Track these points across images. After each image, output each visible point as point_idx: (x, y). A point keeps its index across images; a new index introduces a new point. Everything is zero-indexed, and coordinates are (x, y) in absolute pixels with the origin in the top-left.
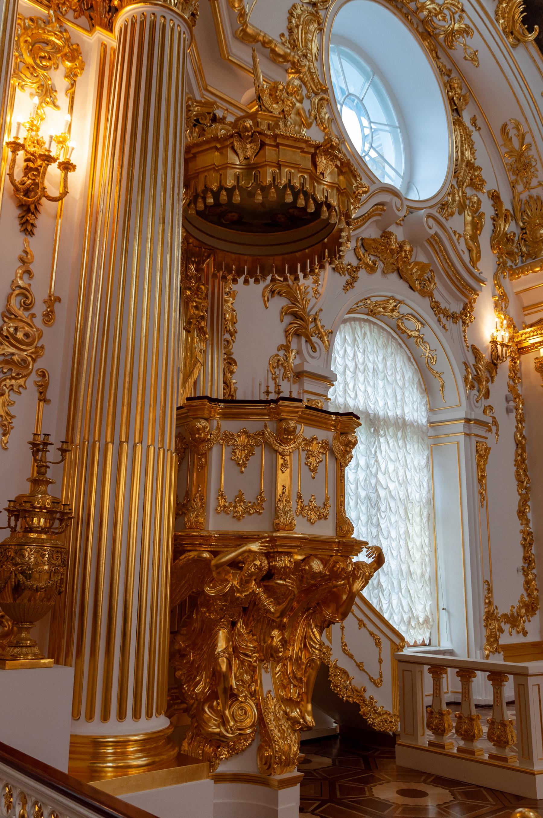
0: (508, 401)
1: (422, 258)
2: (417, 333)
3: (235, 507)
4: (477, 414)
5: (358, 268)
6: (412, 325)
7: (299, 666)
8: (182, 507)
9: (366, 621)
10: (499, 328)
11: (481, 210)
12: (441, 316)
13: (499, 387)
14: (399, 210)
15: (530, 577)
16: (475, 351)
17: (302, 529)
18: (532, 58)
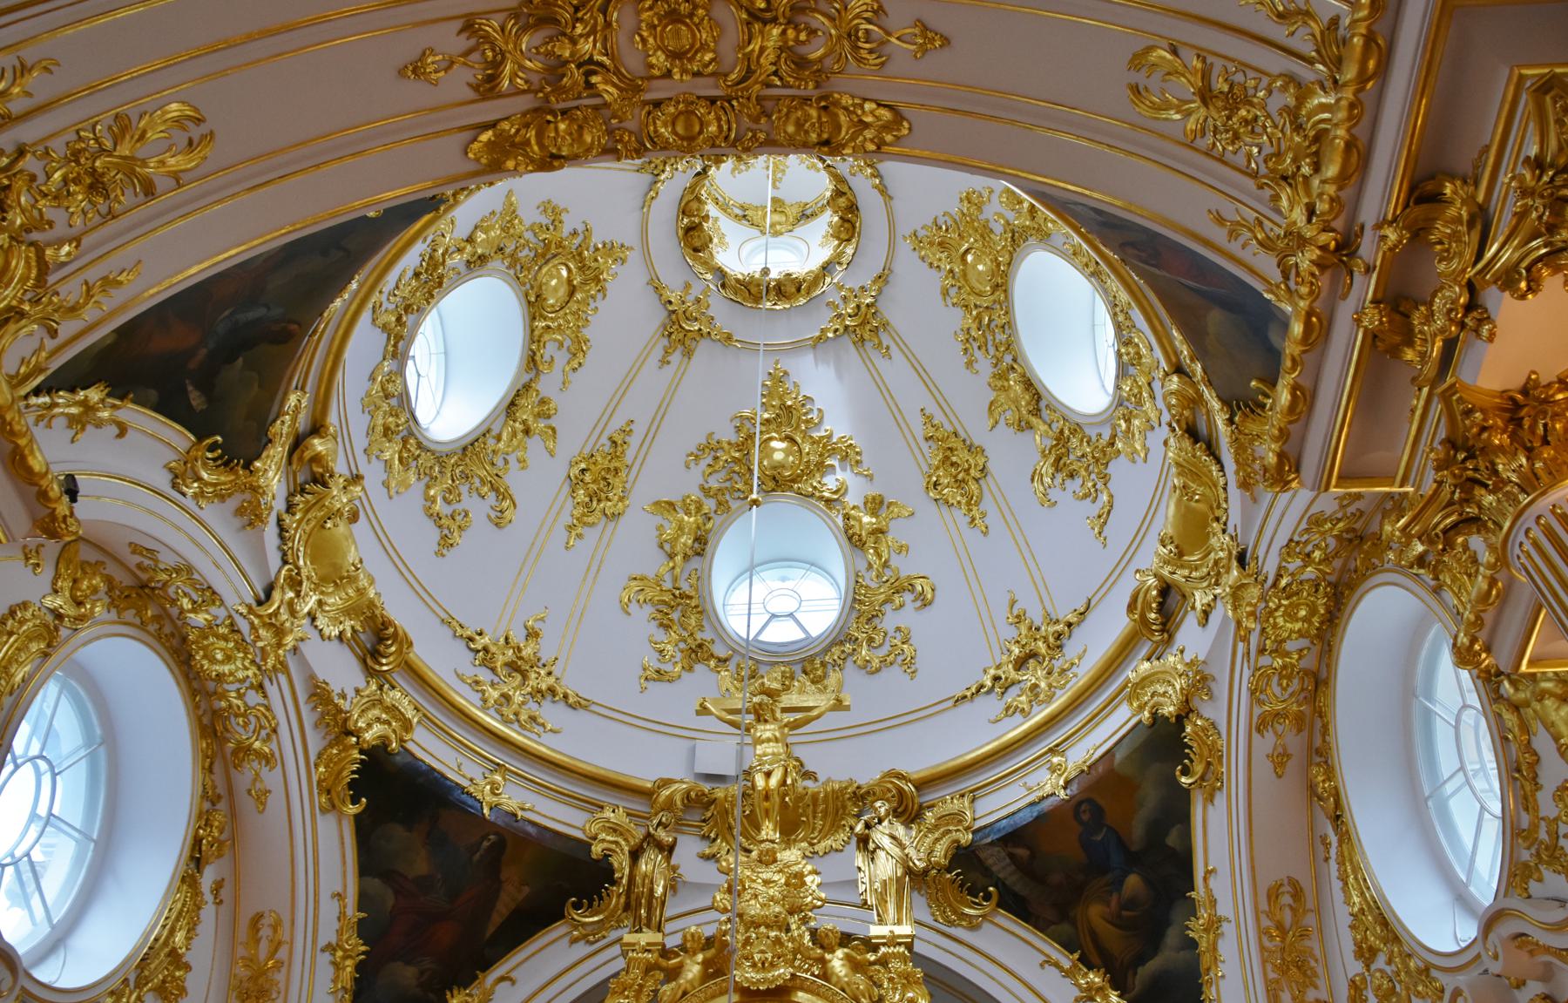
18: (342, 838)
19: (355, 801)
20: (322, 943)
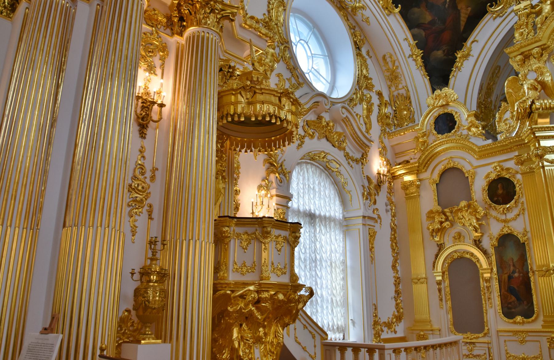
0: (387, 205)
1: (339, 130)
2: (337, 170)
3: (242, 269)
4: (370, 213)
5: (304, 136)
6: (334, 165)
7: (272, 346)
8: (217, 269)
9: (307, 325)
10: (382, 165)
11: (372, 102)
12: (350, 160)
13: (382, 198)
14: (326, 105)
15: (399, 301)
16: (369, 179)
17: (274, 279)
18: (398, 21)
19: (397, 7)
20: (407, 55)
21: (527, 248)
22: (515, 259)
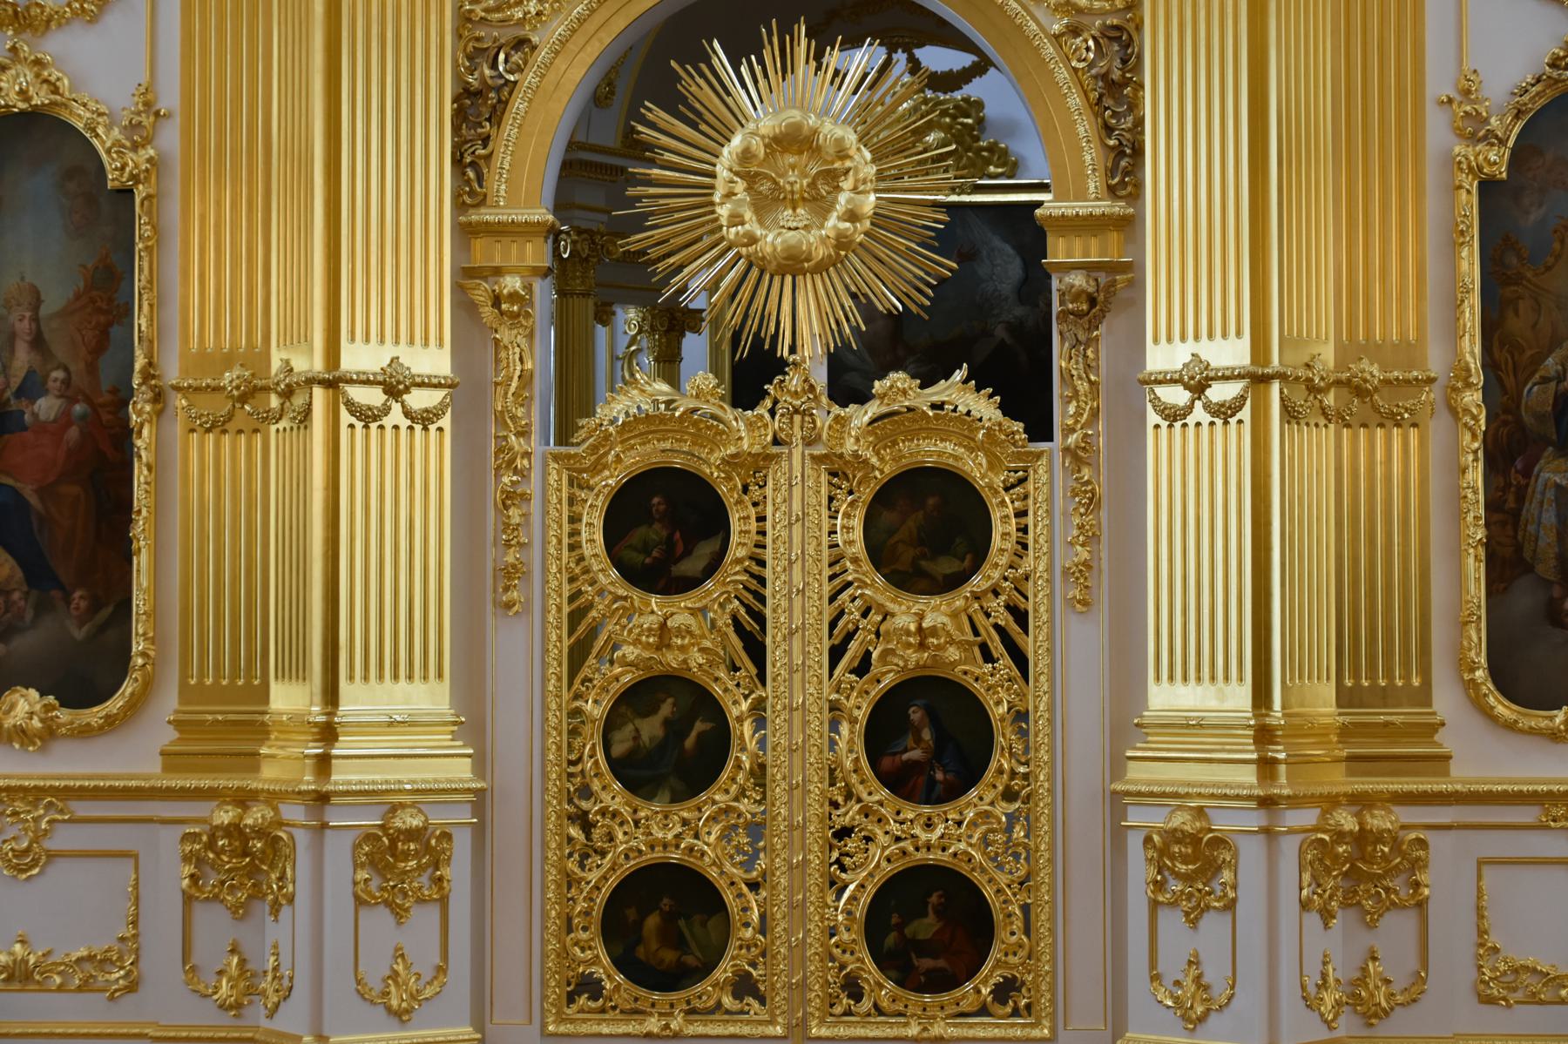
21: (143, 228)
22: (54, 301)
